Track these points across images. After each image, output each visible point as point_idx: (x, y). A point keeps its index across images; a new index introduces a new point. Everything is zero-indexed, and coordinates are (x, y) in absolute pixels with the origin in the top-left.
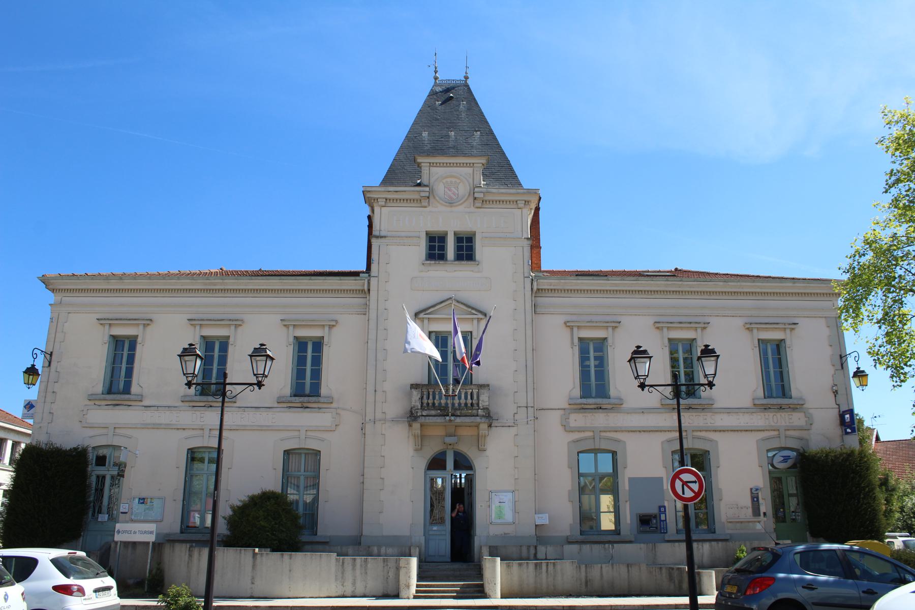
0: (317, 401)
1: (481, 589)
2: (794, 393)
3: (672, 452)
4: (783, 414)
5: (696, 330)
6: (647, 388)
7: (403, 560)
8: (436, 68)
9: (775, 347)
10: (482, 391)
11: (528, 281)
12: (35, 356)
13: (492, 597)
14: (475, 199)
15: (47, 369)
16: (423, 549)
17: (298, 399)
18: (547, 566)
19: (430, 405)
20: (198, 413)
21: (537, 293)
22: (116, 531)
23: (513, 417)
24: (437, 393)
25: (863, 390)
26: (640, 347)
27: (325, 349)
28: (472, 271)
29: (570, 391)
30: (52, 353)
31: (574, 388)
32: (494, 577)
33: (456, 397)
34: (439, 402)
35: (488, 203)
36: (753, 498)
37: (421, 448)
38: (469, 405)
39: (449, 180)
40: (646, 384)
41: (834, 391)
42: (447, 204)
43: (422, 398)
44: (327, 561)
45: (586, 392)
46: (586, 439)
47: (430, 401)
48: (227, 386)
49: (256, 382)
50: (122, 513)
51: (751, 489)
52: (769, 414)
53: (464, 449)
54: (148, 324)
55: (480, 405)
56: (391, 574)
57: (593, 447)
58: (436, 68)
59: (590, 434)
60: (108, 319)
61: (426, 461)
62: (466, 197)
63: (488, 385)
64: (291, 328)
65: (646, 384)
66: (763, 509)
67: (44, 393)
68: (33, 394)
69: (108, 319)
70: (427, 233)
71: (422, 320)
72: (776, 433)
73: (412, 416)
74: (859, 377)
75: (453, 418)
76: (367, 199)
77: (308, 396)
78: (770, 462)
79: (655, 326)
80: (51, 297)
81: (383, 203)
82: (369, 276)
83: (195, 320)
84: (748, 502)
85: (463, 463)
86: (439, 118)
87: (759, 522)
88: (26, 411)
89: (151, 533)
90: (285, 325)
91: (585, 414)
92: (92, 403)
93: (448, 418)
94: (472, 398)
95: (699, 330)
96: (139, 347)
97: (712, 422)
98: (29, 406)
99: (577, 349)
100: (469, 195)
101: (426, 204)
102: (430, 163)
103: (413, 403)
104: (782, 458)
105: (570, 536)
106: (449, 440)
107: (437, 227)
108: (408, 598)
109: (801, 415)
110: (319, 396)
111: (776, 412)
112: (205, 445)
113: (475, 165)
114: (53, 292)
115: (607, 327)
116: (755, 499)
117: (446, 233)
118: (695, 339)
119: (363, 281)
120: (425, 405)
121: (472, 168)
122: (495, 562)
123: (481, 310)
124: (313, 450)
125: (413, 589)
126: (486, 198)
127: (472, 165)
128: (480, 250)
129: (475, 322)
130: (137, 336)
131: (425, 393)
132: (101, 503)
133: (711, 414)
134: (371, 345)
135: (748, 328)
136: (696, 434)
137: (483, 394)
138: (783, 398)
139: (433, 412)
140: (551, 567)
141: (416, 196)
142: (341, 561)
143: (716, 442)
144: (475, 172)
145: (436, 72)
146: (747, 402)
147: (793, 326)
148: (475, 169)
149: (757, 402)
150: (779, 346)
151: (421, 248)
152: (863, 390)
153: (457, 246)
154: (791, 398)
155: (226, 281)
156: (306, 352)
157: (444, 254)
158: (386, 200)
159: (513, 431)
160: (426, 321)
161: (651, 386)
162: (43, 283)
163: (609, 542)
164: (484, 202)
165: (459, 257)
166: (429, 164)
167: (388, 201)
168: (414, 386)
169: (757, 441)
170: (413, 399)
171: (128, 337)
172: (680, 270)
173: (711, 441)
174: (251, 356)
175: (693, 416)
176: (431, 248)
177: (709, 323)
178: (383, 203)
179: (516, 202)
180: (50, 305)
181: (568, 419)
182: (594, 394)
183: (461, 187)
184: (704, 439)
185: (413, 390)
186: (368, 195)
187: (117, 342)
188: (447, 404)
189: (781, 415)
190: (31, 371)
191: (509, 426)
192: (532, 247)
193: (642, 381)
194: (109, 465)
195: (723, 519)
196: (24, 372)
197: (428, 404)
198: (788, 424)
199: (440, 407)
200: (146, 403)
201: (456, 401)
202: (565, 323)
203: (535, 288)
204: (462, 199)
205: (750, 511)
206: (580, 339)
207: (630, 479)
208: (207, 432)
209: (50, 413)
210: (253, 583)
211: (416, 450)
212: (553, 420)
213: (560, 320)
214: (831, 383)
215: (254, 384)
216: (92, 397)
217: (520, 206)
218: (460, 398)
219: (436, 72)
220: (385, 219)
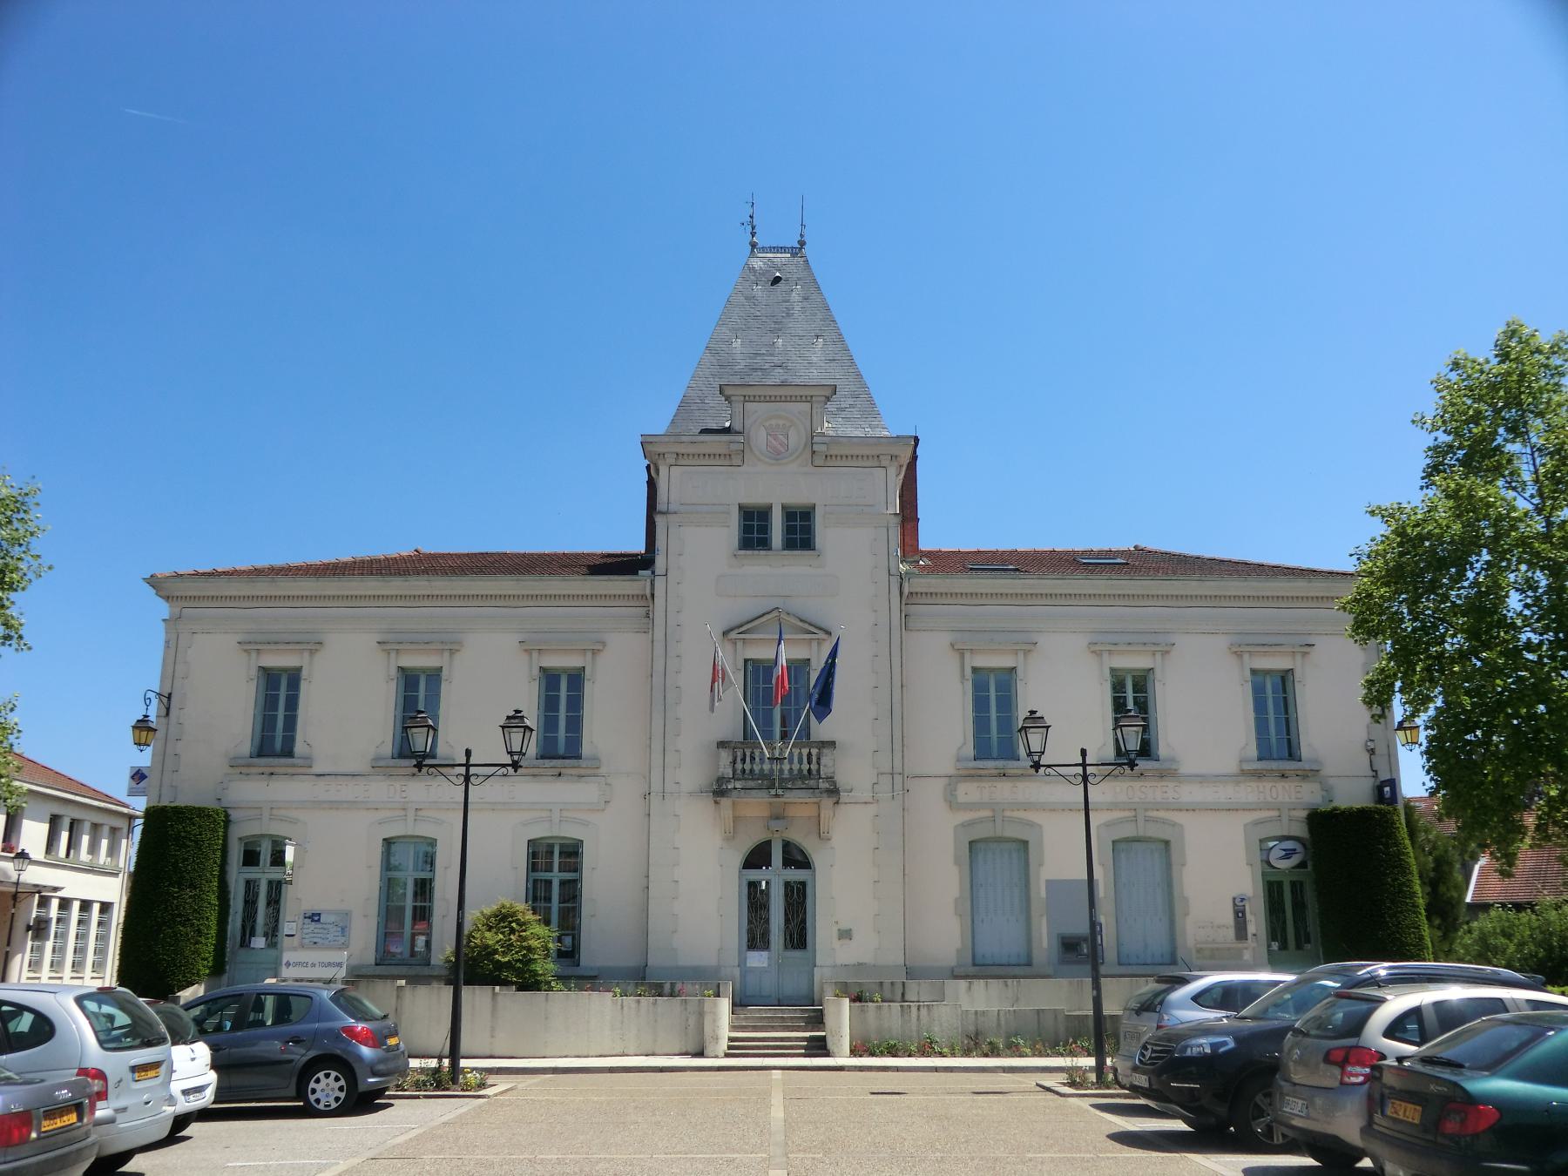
0: (576, 765)
1: (823, 1043)
2: (1305, 752)
3: (1113, 842)
4: (1286, 785)
5: (1154, 654)
6: (1042, 769)
7: (709, 1001)
8: (753, 228)
11: (895, 581)
12: (148, 701)
13: (837, 1055)
14: (814, 452)
15: (163, 720)
16: (738, 985)
17: (548, 763)
19: (747, 772)
20: (397, 785)
22: (284, 961)
23: (871, 788)
25: (1411, 750)
27: (588, 686)
28: (810, 566)
29: (959, 748)
30: (170, 694)
31: (965, 744)
33: (786, 761)
36: (1236, 913)
37: (734, 837)
38: (805, 772)
39: (773, 422)
40: (1041, 763)
41: (1369, 748)
43: (734, 762)
44: (600, 1005)
45: (983, 750)
46: (981, 821)
47: (747, 766)
48: (471, 768)
49: (511, 762)
50: (287, 935)
51: (1234, 899)
52: (1264, 784)
53: (797, 836)
54: (316, 650)
55: (821, 773)
56: (692, 1021)
57: (991, 834)
58: (753, 228)
59: (986, 813)
60: (256, 643)
61: (741, 857)
64: (535, 655)
65: (1041, 763)
66: (1251, 929)
67: (161, 758)
68: (144, 759)
69: (256, 643)
70: (741, 507)
71: (734, 642)
72: (1275, 813)
73: (719, 791)
74: (1405, 729)
75: (780, 792)
77: (564, 758)
78: (1265, 858)
79: (1089, 648)
80: (163, 609)
81: (673, 461)
82: (653, 573)
84: (1229, 918)
85: (796, 858)
86: (758, 314)
87: (1246, 948)
88: (134, 784)
89: (339, 965)
90: (526, 650)
92: (238, 770)
94: (809, 762)
95: (1158, 656)
96: (303, 686)
97: (1176, 796)
98: (139, 776)
99: (969, 685)
100: (804, 449)
105: (956, 967)
106: (775, 825)
107: (756, 498)
108: (716, 1057)
109: (1315, 787)
110: (579, 757)
111: (1276, 782)
112: (410, 833)
113: (814, 398)
115: (1016, 652)
117: (770, 507)
119: (643, 582)
120: (739, 772)
121: (809, 404)
122: (839, 1005)
123: (823, 626)
124: (575, 839)
125: (724, 1045)
126: (833, 452)
127: (809, 398)
128: (823, 533)
129: (814, 644)
130: (299, 669)
131: (739, 754)
132: (255, 921)
133: (1174, 784)
134: (658, 679)
136: (1150, 814)
137: (826, 756)
138: (1289, 760)
139: (751, 784)
140: (924, 1011)
141: (723, 451)
142: (619, 1003)
144: (814, 411)
145: (753, 234)
146: (1232, 767)
148: (815, 406)
149: (1246, 767)
150: (1285, 679)
151: (731, 531)
152: (1411, 750)
153: (787, 526)
154: (1300, 761)
158: (677, 454)
159: (872, 809)
160: (739, 644)
161: (1049, 766)
162: (153, 586)
163: (1014, 977)
164: (829, 458)
166: (742, 398)
168: (722, 744)
169: (1245, 825)
171: (285, 670)
172: (1142, 550)
173: (1174, 825)
174: (503, 727)
176: (746, 529)
177: (1174, 644)
178: (673, 461)
180: (164, 620)
181: (955, 790)
182: (995, 753)
183: (792, 433)
184: (1164, 822)
185: (720, 749)
187: (270, 678)
188: (772, 770)
189: (1283, 787)
190: (142, 726)
191: (866, 803)
193: (1036, 758)
195: (1190, 942)
196: (133, 727)
197: (744, 771)
198: (1293, 800)
199: (762, 776)
200: (317, 769)
201: (786, 767)
202: (952, 645)
203: (906, 591)
204: (797, 450)
205: (1231, 933)
206: (975, 670)
207: (1047, 881)
208: (411, 814)
209: (172, 786)
210: (492, 1037)
211: (727, 839)
212: (930, 795)
213: (944, 639)
214: (1364, 736)
215: (509, 765)
216: (235, 763)
217: (883, 464)
218: (791, 762)
219: (753, 234)
220: (674, 484)
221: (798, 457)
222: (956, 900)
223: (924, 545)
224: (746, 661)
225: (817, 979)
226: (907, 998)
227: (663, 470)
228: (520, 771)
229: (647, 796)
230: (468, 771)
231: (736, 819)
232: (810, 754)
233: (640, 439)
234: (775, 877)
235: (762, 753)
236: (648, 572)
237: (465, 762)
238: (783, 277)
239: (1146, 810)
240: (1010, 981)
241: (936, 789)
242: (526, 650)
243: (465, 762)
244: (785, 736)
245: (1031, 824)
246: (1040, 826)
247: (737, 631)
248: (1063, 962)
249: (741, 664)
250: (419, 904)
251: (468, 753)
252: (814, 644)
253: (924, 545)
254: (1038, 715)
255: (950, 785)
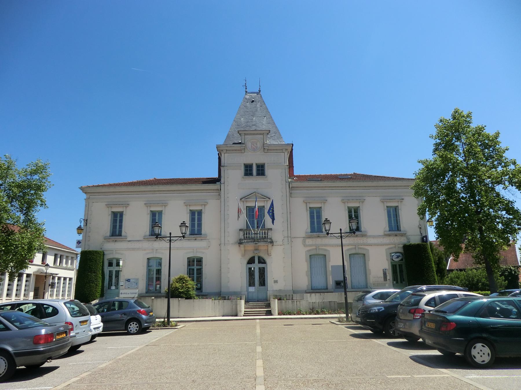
1: (270, 312)
2: (402, 229)
5: (360, 203)
6: (329, 234)
9: (394, 209)
10: (269, 231)
14: (264, 149)
15: (85, 227)
16: (246, 296)
17: (192, 236)
18: (297, 302)
19: (248, 237)
21: (291, 188)
23: (282, 241)
24: (250, 232)
26: (327, 219)
30: (87, 219)
32: (275, 307)
34: (251, 236)
35: (270, 150)
36: (384, 273)
39: (253, 141)
42: (253, 151)
43: (244, 235)
44: (208, 303)
45: (313, 230)
46: (313, 249)
47: (248, 236)
50: (121, 286)
51: (383, 270)
52: (391, 238)
53: (262, 255)
56: (234, 307)
57: (316, 253)
59: (314, 247)
62: (260, 149)
63: (272, 229)
66: (388, 278)
67: (85, 237)
68: (80, 238)
73: (240, 243)
74: (429, 222)
75: (257, 243)
76: (218, 150)
78: (391, 258)
80: (84, 196)
81: (225, 152)
82: (221, 183)
83: (147, 204)
84: (382, 275)
85: (262, 261)
89: (136, 293)
91: (312, 239)
92: (106, 240)
93: (255, 243)
96: (124, 216)
98: (79, 242)
100: (262, 148)
101: (244, 152)
102: (245, 134)
103: (240, 237)
104: (397, 257)
106: (256, 252)
107: (248, 162)
114: (86, 194)
116: (385, 274)
118: (359, 207)
120: (245, 237)
125: (243, 313)
126: (270, 149)
127: (263, 134)
128: (267, 171)
129: (266, 202)
134: (222, 212)
135: (382, 202)
136: (359, 247)
139: (249, 241)
140: (298, 303)
141: (239, 149)
143: (368, 250)
144: (264, 137)
147: (402, 200)
149: (386, 233)
150: (396, 209)
155: (160, 187)
156: (195, 216)
157: (252, 173)
159: (282, 247)
160: (245, 202)
165: (258, 174)
167: (227, 151)
168: (240, 230)
169: (386, 250)
170: (241, 235)
171: (119, 212)
173: (366, 249)
174: (180, 226)
175: (358, 239)
179: (282, 149)
180: (85, 199)
183: (258, 144)
184: (363, 249)
185: (240, 231)
186: (219, 148)
190: (79, 229)
192: (289, 168)
193: (328, 232)
194: (114, 266)
197: (247, 237)
198: (399, 242)
199: (252, 238)
200: (128, 239)
201: (258, 236)
202: (304, 201)
203: (291, 186)
205: (383, 279)
206: (310, 208)
207: (331, 266)
210: (179, 312)
212: (298, 243)
214: (418, 224)
215: (182, 237)
216: (106, 238)
217: (283, 151)
218: (260, 234)
220: (225, 158)
221: (261, 149)
222: (306, 271)
223: (295, 174)
224: (247, 207)
225: (268, 294)
226: (293, 299)
227: (223, 155)
228: (185, 238)
229: (220, 245)
230: (170, 239)
231: (245, 250)
232: (265, 232)
233: (216, 146)
234: (256, 266)
235: (252, 232)
236: (219, 183)
237: (169, 236)
238: (255, 100)
239: (358, 246)
240: (322, 293)
241: (300, 241)
242: (186, 205)
243: (169, 236)
244: (258, 227)
245: (326, 250)
246: (329, 251)
247: (244, 198)
248: (336, 288)
249: (245, 208)
250: (157, 276)
251: (170, 234)
252: (266, 202)
253: (295, 174)
254: (328, 220)
255: (304, 240)
